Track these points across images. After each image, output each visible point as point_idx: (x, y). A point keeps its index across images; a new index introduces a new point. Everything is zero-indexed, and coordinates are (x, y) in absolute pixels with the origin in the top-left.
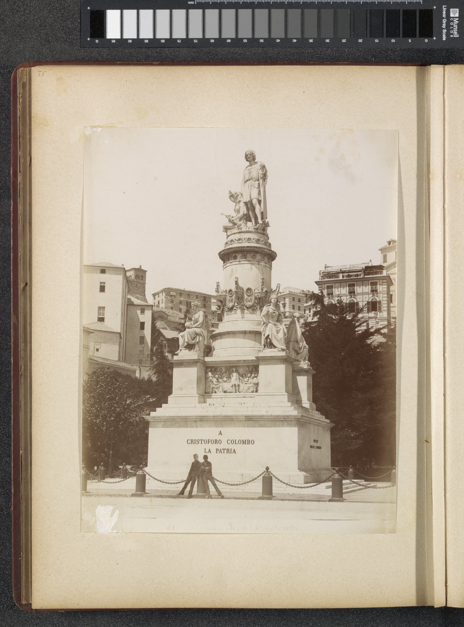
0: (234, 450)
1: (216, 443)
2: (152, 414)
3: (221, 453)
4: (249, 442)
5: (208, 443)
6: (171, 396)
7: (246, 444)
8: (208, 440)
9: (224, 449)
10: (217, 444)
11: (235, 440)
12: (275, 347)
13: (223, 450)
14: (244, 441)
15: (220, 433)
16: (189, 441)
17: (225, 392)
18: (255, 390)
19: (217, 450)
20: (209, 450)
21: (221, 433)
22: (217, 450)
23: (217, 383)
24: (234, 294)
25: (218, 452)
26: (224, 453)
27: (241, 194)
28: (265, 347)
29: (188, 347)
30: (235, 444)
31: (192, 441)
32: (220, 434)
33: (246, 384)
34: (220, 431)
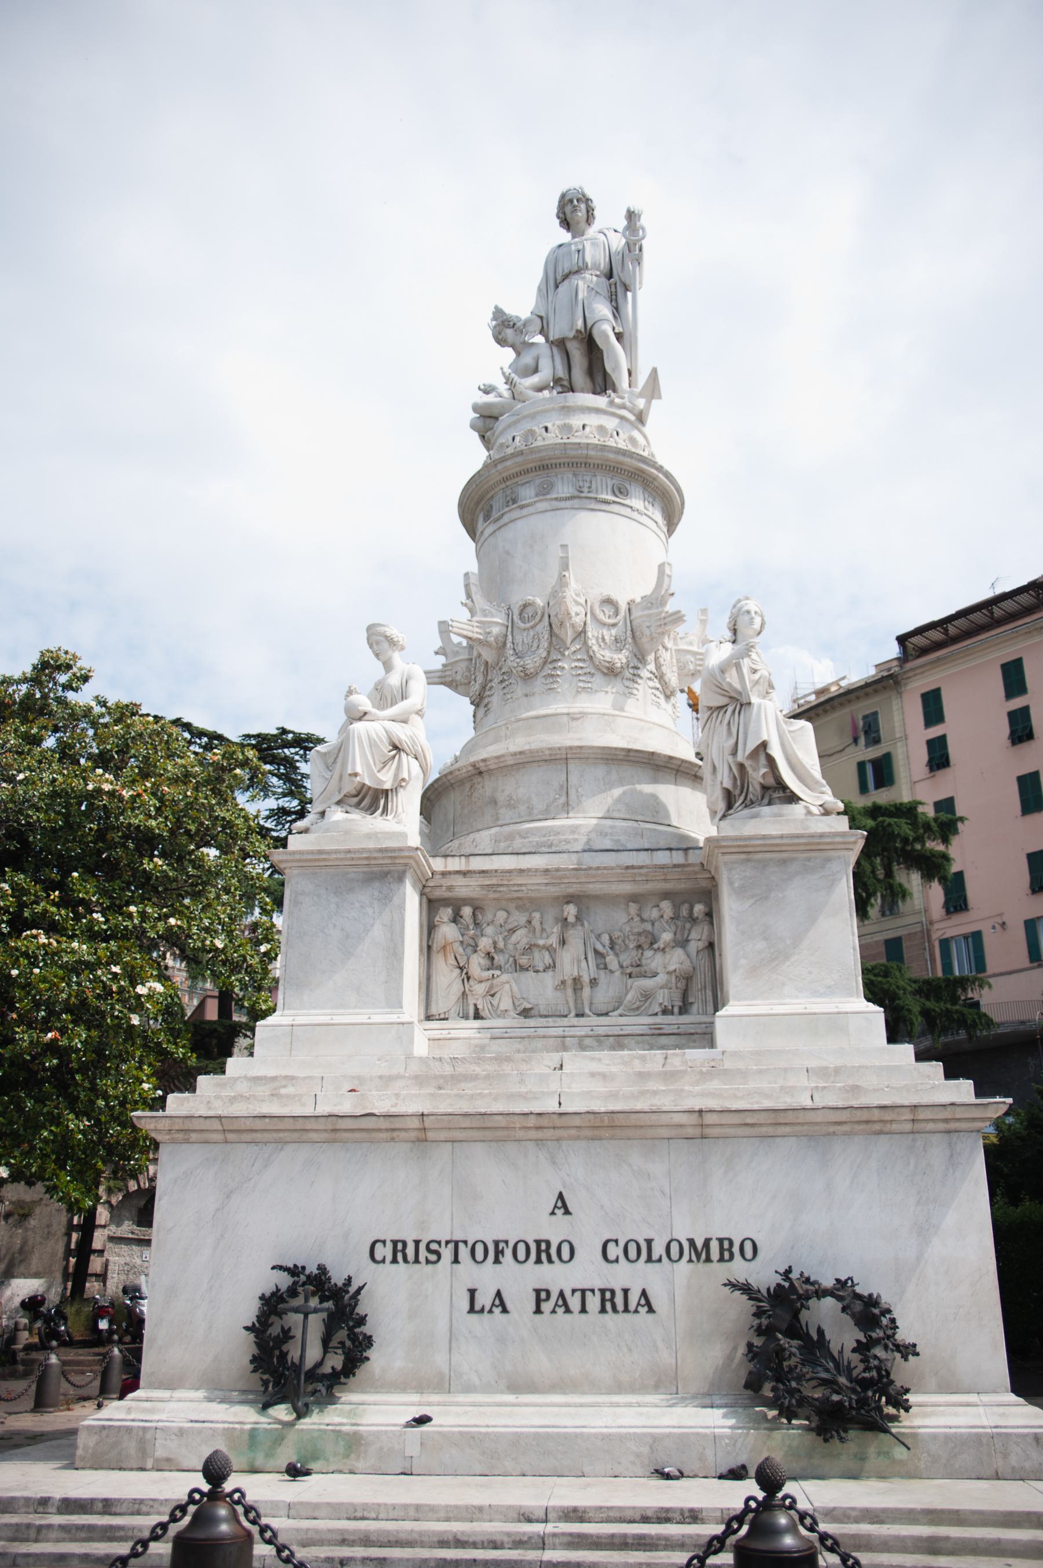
0: (644, 1293)
1: (544, 1256)
2: (177, 1103)
3: (568, 1310)
4: (730, 1250)
5: (497, 1261)
6: (270, 1020)
7: (708, 1260)
8: (496, 1243)
9: (583, 1292)
10: (550, 1260)
11: (649, 1242)
12: (793, 798)
13: (578, 1294)
14: (699, 1244)
15: (562, 1205)
16: (379, 1246)
17: (526, 1013)
18: (678, 1003)
19: (543, 1295)
20: (499, 1294)
21: (565, 1206)
22: (543, 1295)
23: (491, 972)
24: (543, 616)
25: (547, 1307)
26: (583, 1310)
27: (541, 318)
28: (730, 806)
29: (356, 800)
30: (649, 1259)
31: (400, 1246)
32: (560, 1212)
33: (630, 976)
34: (561, 1196)
